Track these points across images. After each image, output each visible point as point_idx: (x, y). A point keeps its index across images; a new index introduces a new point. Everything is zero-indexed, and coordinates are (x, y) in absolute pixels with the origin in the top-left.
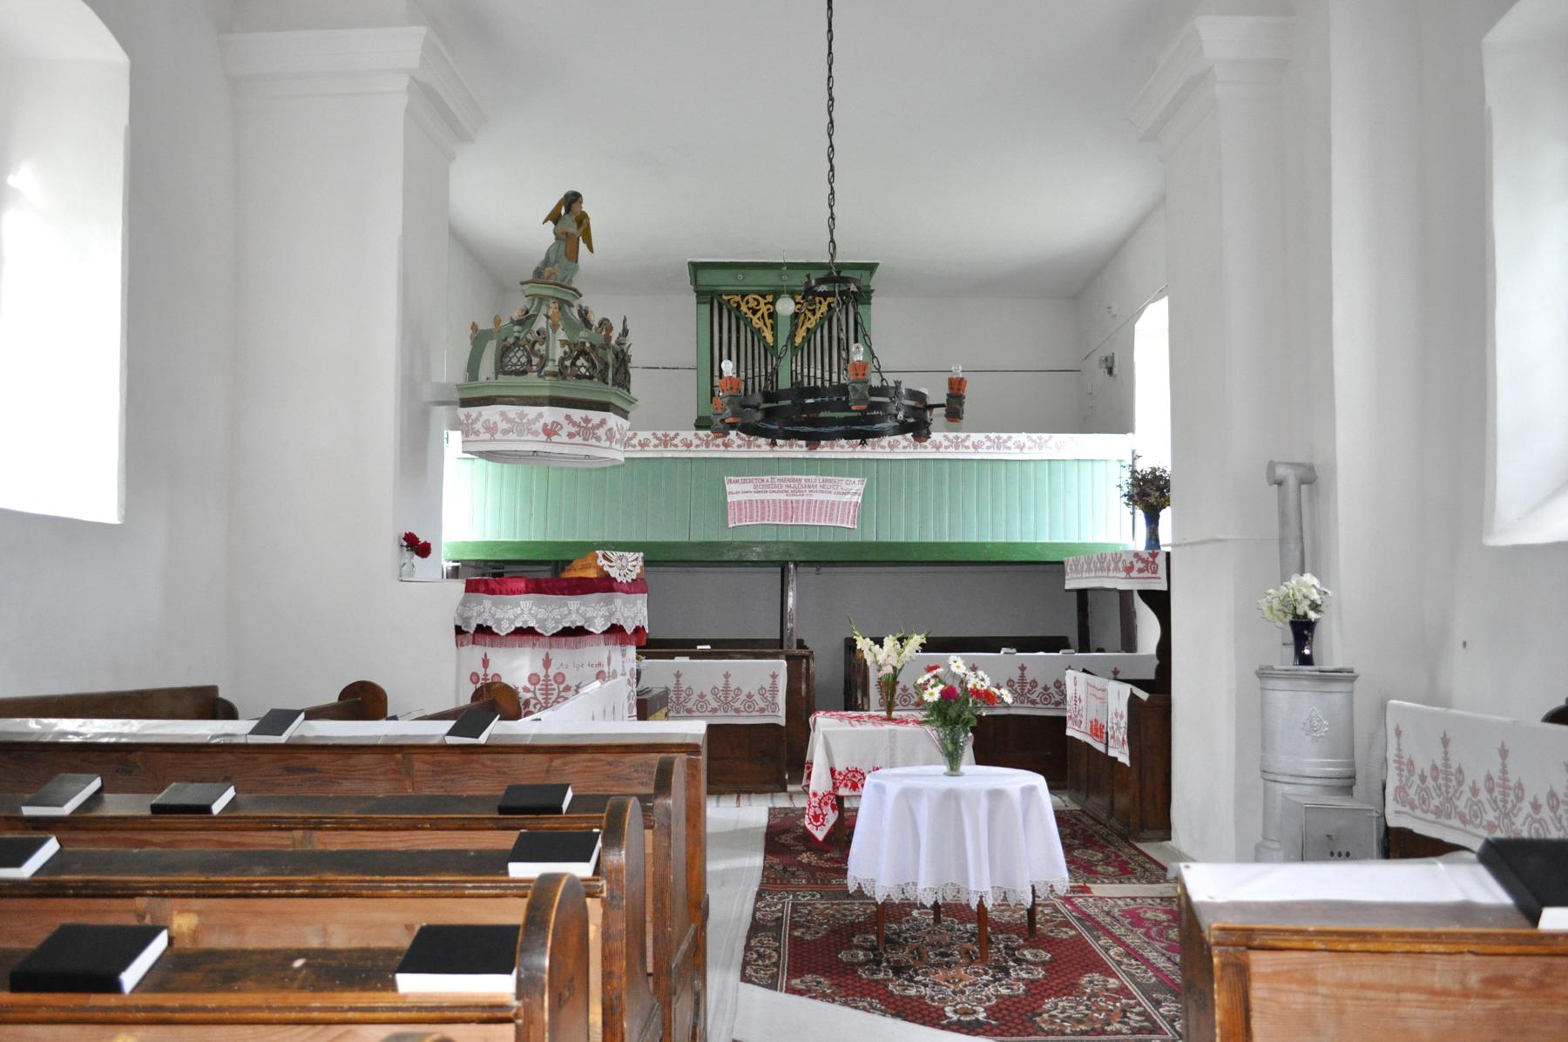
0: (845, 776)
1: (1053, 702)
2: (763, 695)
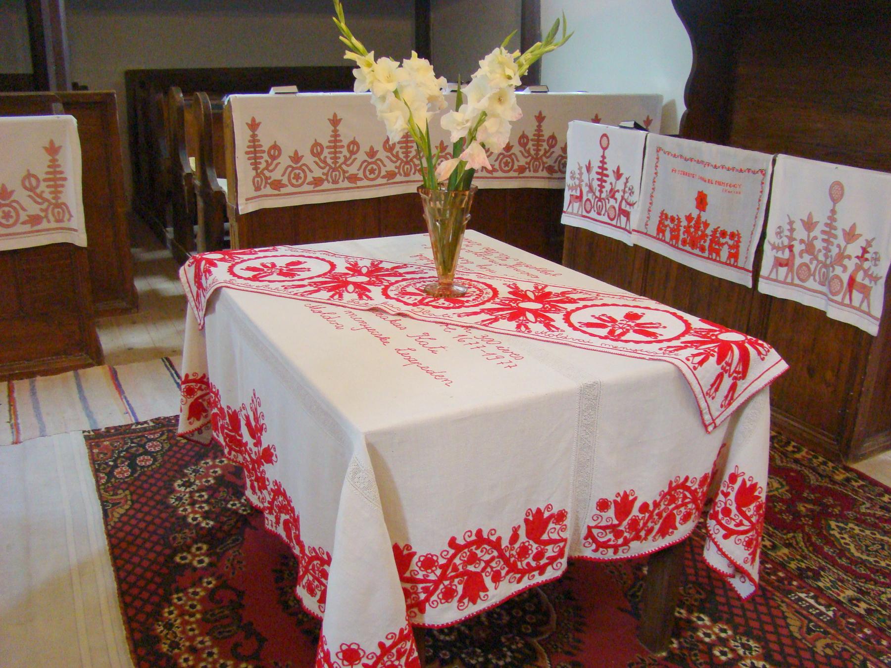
0: (444, 568)
1: (516, 167)
2: (32, 189)
